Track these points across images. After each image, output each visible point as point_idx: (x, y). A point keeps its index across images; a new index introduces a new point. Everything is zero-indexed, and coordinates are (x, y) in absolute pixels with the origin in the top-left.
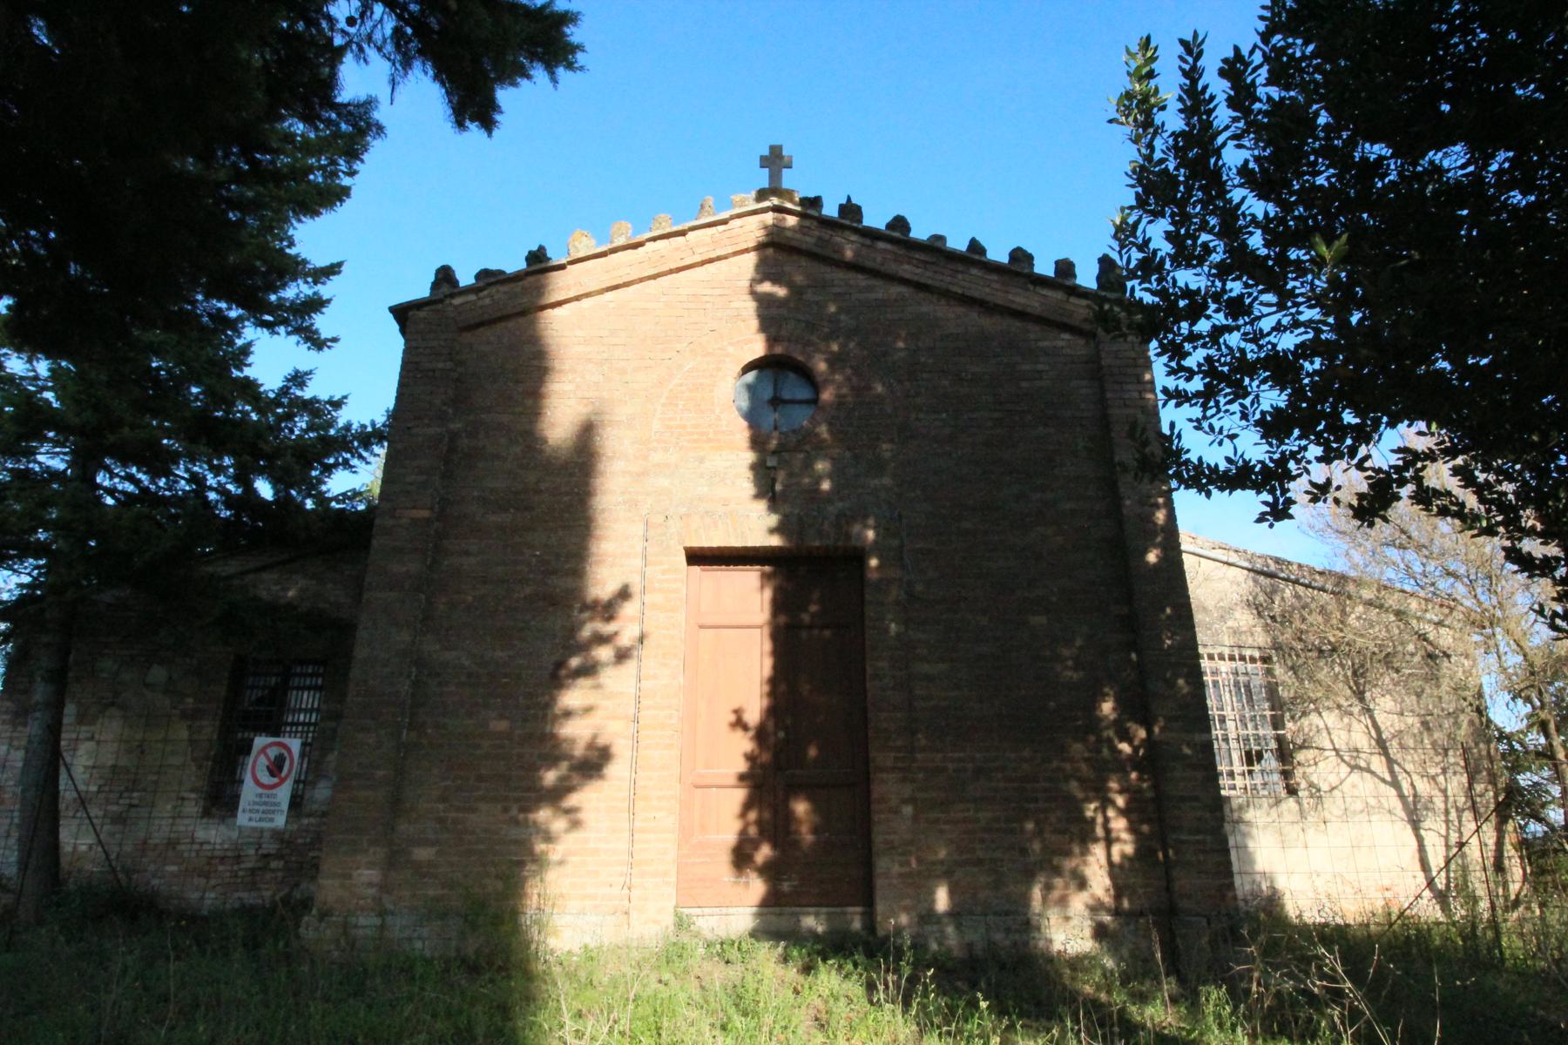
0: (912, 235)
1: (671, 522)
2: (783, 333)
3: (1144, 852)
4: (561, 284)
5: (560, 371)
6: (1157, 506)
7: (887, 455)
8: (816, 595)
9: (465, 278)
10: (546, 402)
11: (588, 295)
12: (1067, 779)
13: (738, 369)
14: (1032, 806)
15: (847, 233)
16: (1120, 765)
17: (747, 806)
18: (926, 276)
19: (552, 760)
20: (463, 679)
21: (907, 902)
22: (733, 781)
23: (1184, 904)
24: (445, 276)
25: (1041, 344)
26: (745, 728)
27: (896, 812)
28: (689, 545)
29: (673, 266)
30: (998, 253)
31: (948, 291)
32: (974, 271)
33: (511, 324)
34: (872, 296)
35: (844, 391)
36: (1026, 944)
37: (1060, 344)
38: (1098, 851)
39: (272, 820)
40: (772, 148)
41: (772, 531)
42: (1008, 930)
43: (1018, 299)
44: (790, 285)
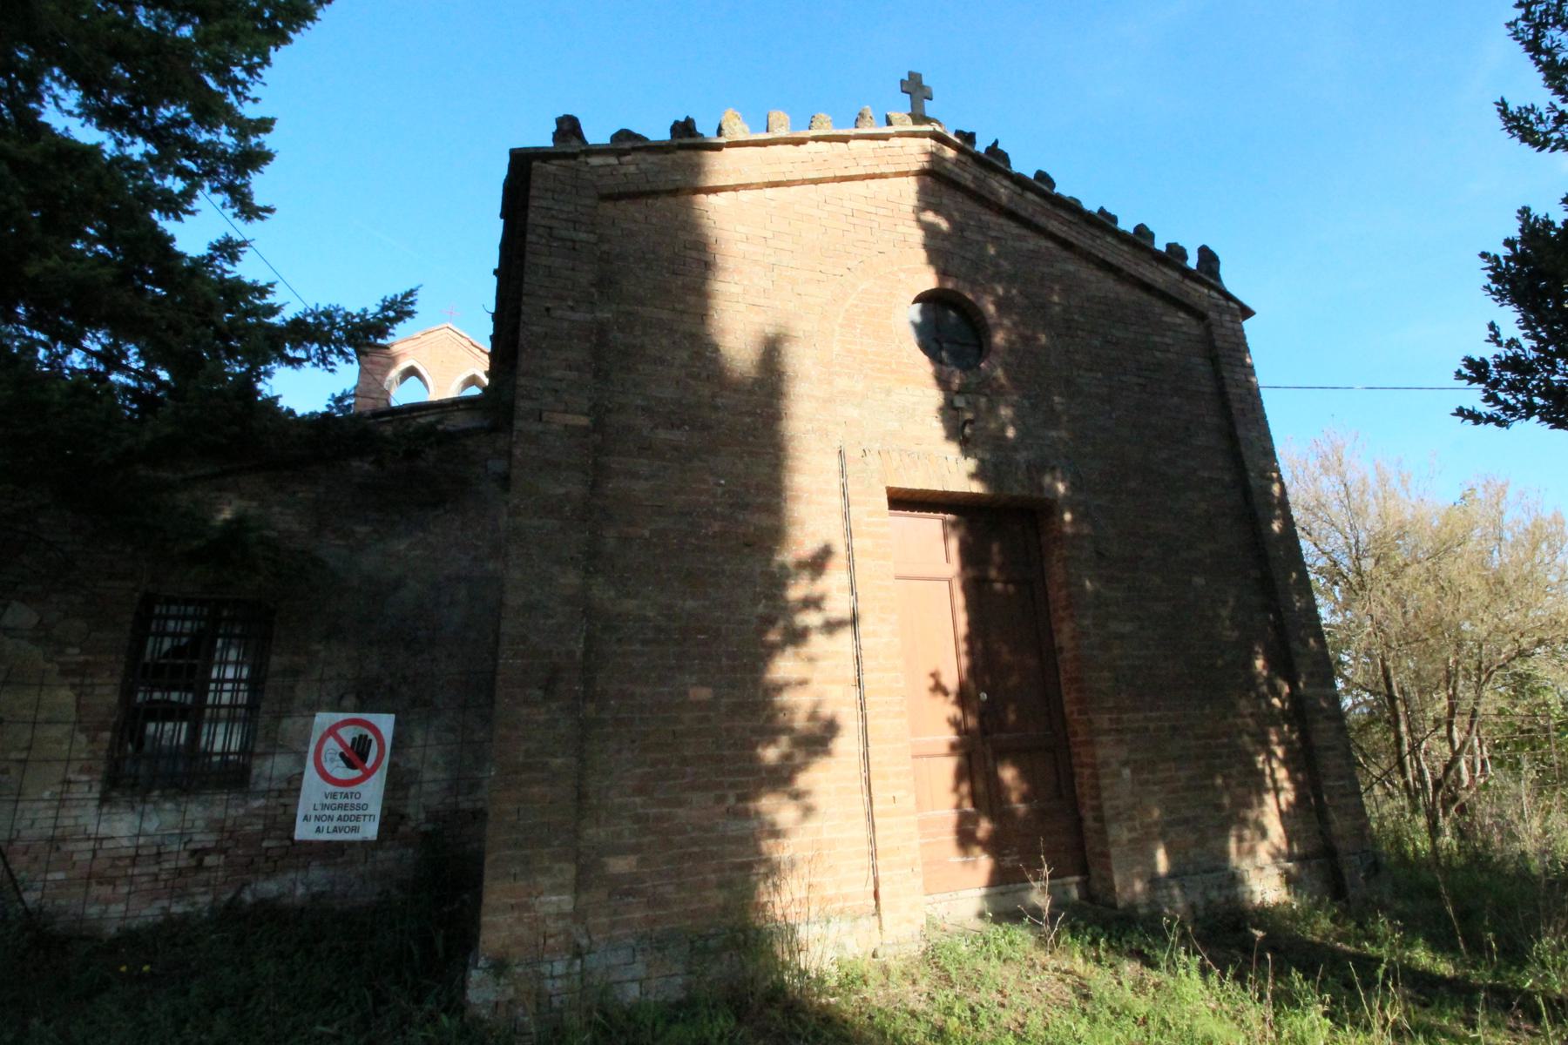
0: (1056, 190)
1: (869, 458)
5: (725, 270)
6: (1272, 480)
8: (995, 548)
9: (597, 133)
10: (713, 302)
11: (746, 187)
12: (1240, 733)
15: (999, 177)
16: (1274, 718)
18: (1071, 235)
19: (771, 732)
20: (650, 635)
21: (1139, 869)
22: (945, 749)
24: (568, 128)
26: (946, 693)
27: (1118, 775)
29: (839, 174)
30: (1126, 225)
31: (1090, 253)
32: (1109, 239)
33: (659, 203)
35: (1013, 337)
37: (1178, 321)
38: (1269, 799)
39: (355, 829)
40: (911, 74)
41: (973, 476)
42: (1220, 887)
44: (949, 218)
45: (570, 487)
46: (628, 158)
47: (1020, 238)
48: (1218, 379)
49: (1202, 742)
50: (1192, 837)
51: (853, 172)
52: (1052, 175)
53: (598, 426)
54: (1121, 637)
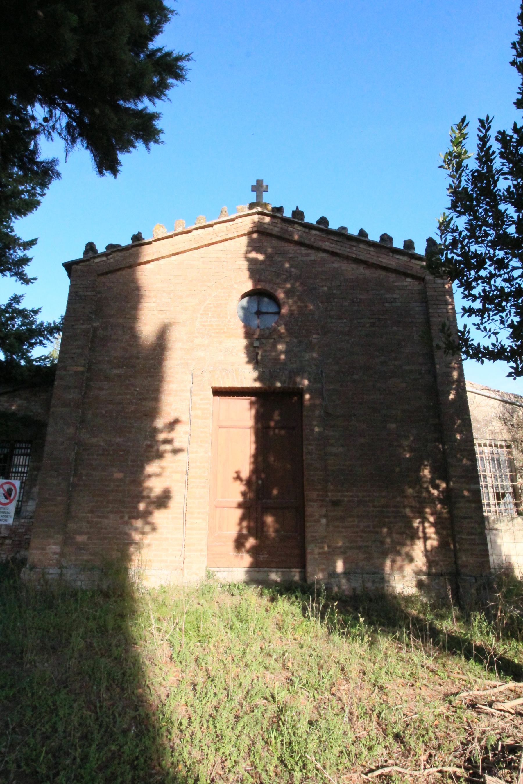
1: (205, 374)
2: (263, 278)
3: (443, 544)
4: (148, 252)
7: (315, 341)
9: (101, 249)
11: (163, 258)
12: (405, 507)
13: (240, 296)
14: (387, 520)
15: (296, 226)
16: (431, 501)
17: (242, 519)
20: (101, 452)
23: (463, 571)
24: (90, 247)
25: (396, 284)
27: (318, 521)
28: (214, 386)
29: (206, 243)
30: (374, 237)
32: (361, 246)
33: (124, 273)
34: (309, 258)
35: (294, 308)
36: (383, 588)
37: (405, 284)
39: (6, 520)
42: (374, 582)
43: (384, 261)
45: (72, 395)
46: (111, 256)
47: (307, 255)
48: (427, 313)
49: (379, 509)
50: (362, 556)
51: (214, 241)
52: (328, 219)
53: (89, 370)
54: (336, 455)
